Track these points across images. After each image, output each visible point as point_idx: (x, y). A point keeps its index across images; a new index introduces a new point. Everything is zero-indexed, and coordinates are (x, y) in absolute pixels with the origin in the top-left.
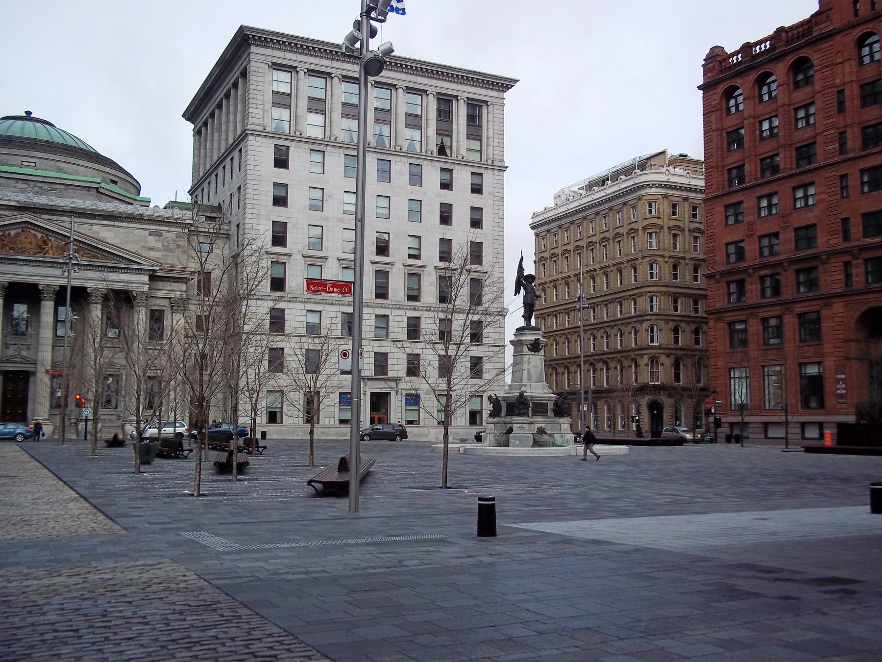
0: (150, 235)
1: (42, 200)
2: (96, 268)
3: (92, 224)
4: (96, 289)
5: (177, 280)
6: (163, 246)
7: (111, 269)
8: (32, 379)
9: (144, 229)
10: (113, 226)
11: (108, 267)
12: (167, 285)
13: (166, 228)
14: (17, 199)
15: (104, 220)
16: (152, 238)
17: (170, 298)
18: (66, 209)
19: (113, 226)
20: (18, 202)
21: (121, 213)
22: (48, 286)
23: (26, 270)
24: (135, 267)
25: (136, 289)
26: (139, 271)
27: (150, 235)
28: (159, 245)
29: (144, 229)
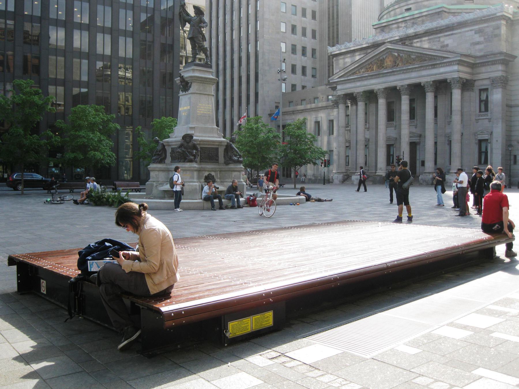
0: (475, 33)
1: (411, 31)
2: (426, 68)
3: (439, 37)
4: (427, 82)
5: (494, 63)
6: (485, 39)
7: (434, 66)
8: (418, 147)
9: (471, 30)
10: (452, 34)
11: (431, 65)
12: (489, 68)
13: (486, 25)
14: (399, 34)
15: (446, 31)
16: (477, 36)
17: (489, 78)
18: (422, 32)
19: (452, 34)
20: (399, 36)
21: (453, 24)
22: (402, 86)
23: (392, 78)
24: (445, 61)
25: (449, 77)
26: (450, 64)
27: (475, 33)
28: (482, 39)
29: (471, 30)
